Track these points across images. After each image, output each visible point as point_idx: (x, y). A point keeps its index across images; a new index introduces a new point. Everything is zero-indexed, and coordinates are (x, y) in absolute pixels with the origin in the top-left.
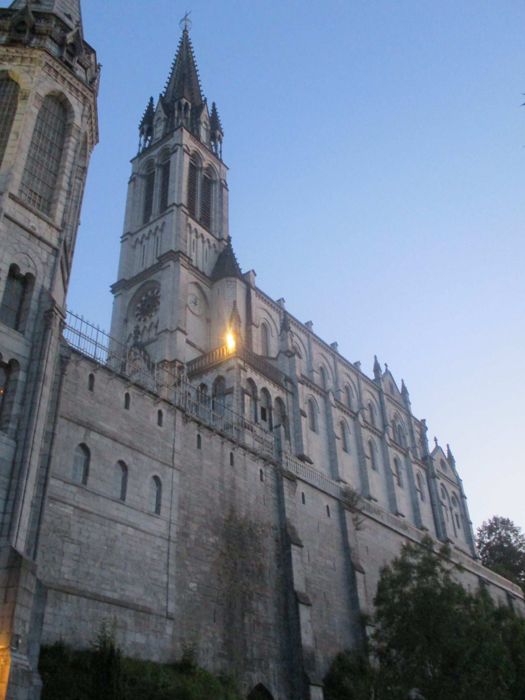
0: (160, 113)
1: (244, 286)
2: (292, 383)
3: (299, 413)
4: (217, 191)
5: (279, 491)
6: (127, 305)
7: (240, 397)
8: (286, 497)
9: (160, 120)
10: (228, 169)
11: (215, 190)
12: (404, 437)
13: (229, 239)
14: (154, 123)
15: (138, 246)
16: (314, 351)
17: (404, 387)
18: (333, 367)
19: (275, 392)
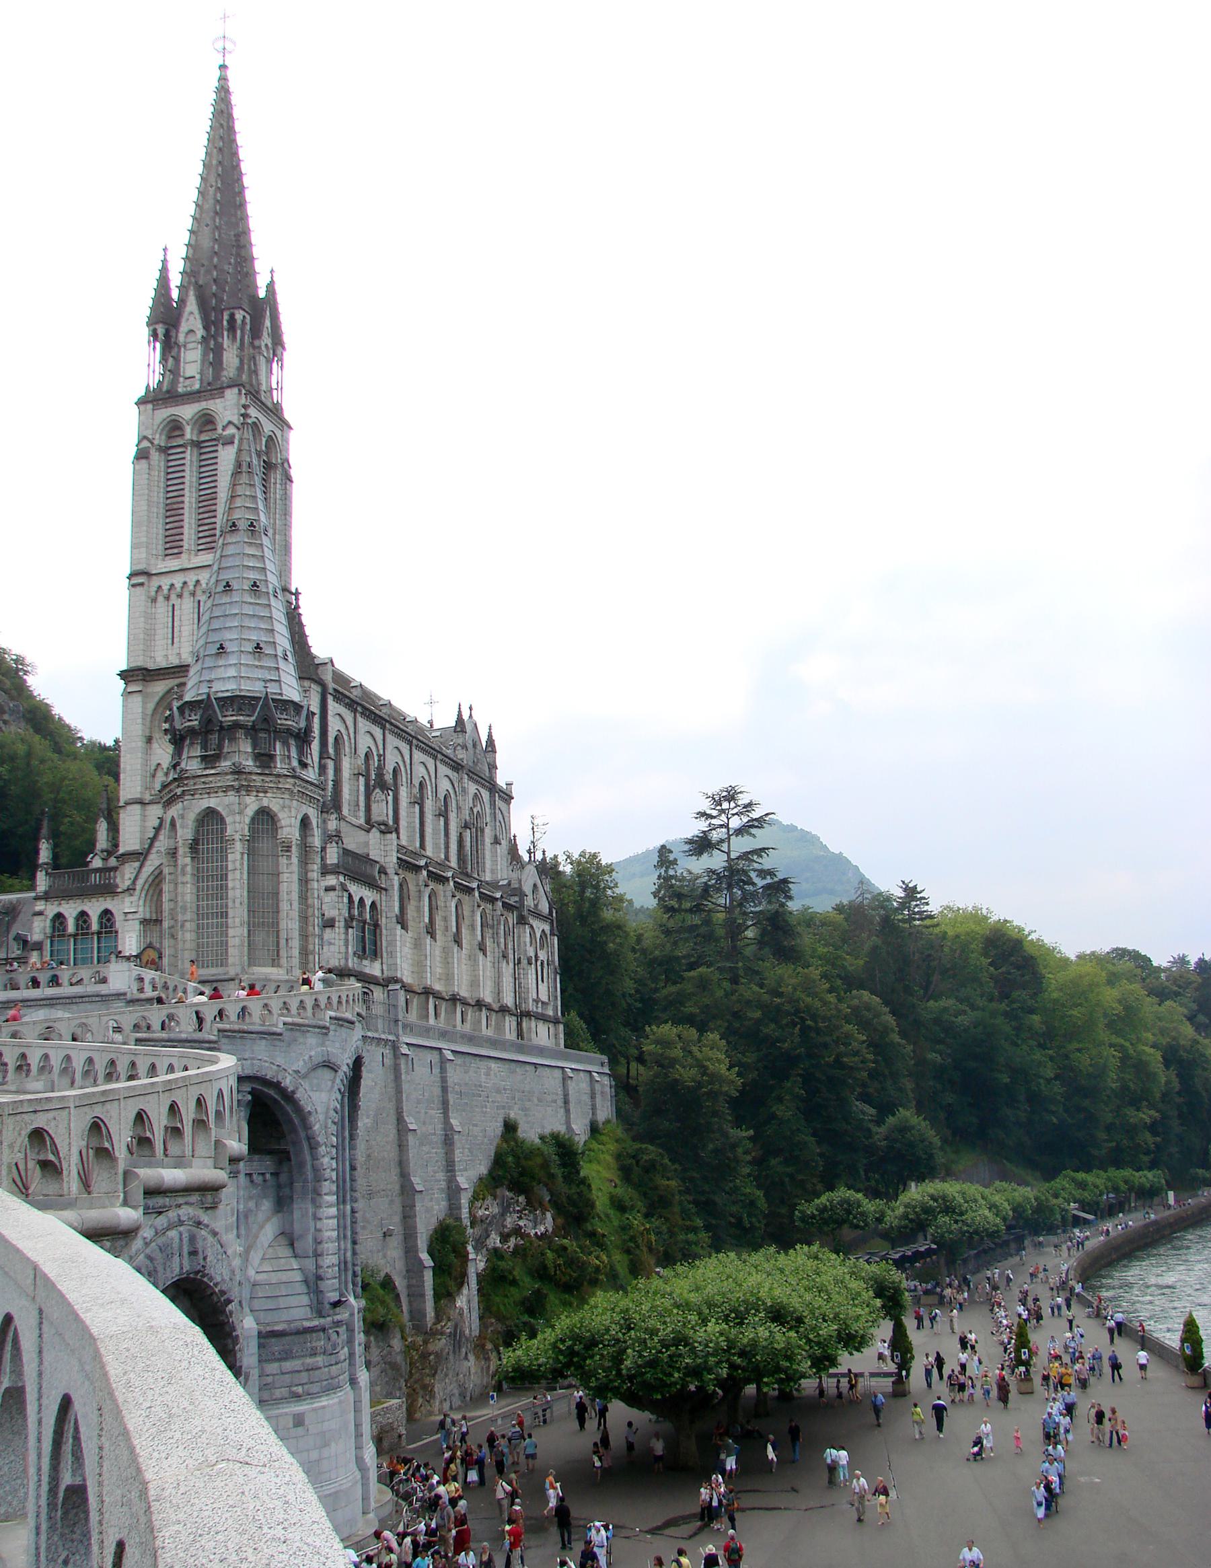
0: (192, 318)
1: (319, 689)
2: (386, 874)
3: (394, 920)
4: (278, 486)
5: (396, 1069)
6: (149, 712)
7: (342, 930)
8: (403, 1077)
9: (191, 338)
10: (290, 428)
11: (275, 483)
12: (482, 831)
13: (297, 594)
14: (181, 338)
15: (160, 599)
16: (389, 748)
17: (491, 741)
18: (408, 762)
19: (369, 896)
